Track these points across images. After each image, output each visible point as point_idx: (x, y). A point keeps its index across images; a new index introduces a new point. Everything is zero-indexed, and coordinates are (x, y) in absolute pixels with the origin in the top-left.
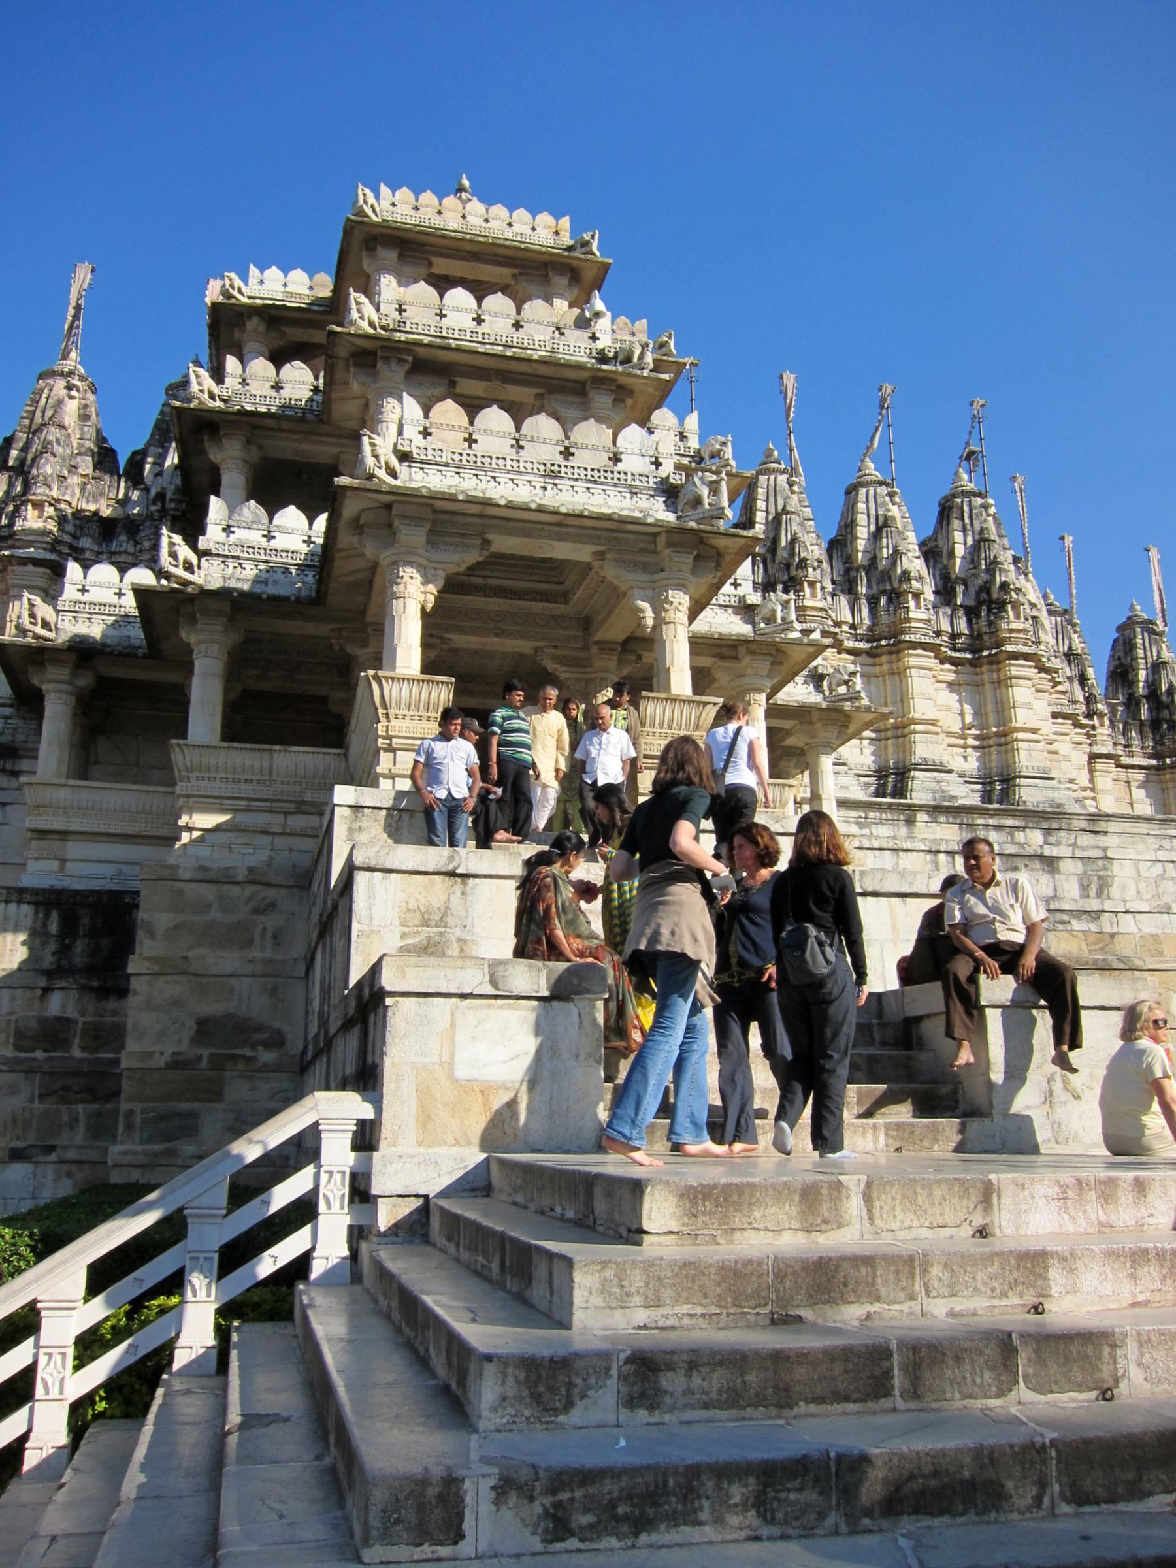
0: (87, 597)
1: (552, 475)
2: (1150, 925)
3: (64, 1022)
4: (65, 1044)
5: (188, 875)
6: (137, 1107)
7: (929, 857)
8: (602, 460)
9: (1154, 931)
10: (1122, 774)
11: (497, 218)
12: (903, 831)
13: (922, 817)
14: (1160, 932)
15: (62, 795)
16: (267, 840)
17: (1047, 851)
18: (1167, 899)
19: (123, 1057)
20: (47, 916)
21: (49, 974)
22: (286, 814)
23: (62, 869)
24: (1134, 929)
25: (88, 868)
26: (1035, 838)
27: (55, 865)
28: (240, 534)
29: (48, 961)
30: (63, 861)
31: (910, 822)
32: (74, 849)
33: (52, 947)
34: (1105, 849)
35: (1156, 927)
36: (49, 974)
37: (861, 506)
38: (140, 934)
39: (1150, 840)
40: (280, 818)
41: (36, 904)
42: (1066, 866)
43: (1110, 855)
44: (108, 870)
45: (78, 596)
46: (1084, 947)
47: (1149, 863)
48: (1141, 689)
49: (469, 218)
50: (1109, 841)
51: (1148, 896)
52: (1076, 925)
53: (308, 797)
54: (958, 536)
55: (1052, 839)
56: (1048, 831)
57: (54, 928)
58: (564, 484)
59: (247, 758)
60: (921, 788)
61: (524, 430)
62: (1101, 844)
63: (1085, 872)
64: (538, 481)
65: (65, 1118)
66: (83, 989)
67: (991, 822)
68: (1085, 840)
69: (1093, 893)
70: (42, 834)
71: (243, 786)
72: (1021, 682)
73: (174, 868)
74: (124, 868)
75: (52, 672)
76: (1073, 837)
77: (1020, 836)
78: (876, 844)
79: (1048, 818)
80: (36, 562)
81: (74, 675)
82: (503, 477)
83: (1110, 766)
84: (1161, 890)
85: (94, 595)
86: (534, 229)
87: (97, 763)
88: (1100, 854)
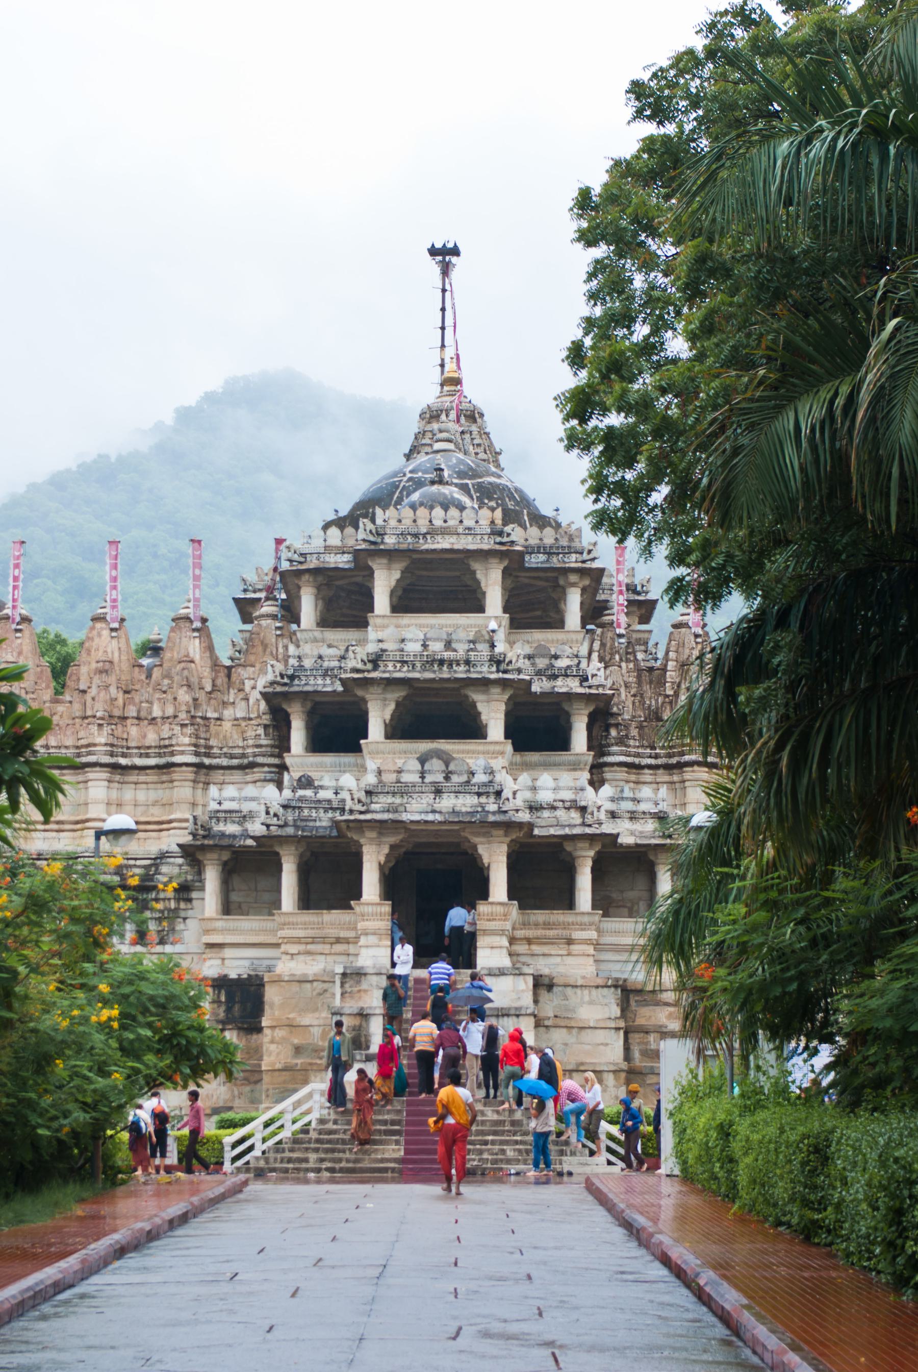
0: (224, 807)
1: (438, 792)
5: (286, 978)
6: (271, 1087)
11: (453, 518)
15: (219, 924)
16: (323, 957)
19: (263, 1063)
20: (219, 993)
21: (223, 1022)
22: (331, 944)
23: (223, 964)
27: (219, 962)
29: (222, 1015)
30: (223, 959)
32: (228, 953)
33: (223, 1008)
36: (223, 1022)
38: (266, 1007)
40: (328, 946)
41: (213, 986)
45: (217, 807)
49: (434, 522)
53: (342, 935)
57: (223, 999)
58: (445, 796)
59: (310, 917)
61: (426, 768)
64: (432, 796)
65: (236, 1093)
66: (239, 1029)
71: (309, 931)
73: (279, 976)
74: (255, 962)
75: (209, 856)
80: (187, 765)
81: (220, 855)
82: (415, 796)
85: (227, 806)
86: (477, 522)
87: (233, 890)
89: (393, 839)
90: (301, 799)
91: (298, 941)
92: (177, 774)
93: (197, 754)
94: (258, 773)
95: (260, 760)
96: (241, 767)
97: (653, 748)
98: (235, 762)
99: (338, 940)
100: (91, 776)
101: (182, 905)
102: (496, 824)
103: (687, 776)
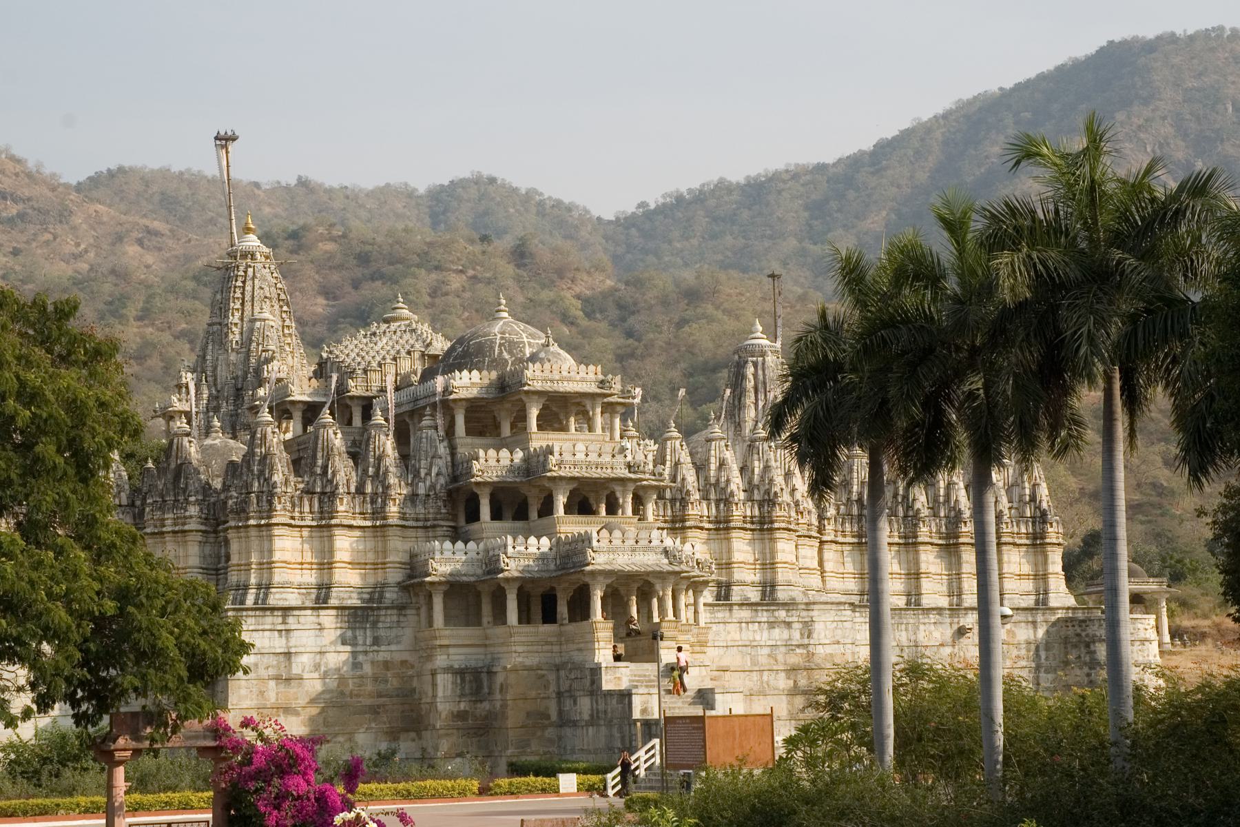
2: (829, 650)
3: (466, 712)
4: (467, 720)
8: (646, 542)
10: (839, 547)
12: (727, 614)
13: (736, 607)
15: (447, 632)
18: (837, 638)
25: (457, 658)
26: (782, 614)
28: (518, 548)
31: (730, 610)
32: (451, 651)
37: (713, 452)
42: (796, 626)
44: (463, 657)
50: (815, 613)
52: (798, 651)
54: (756, 463)
60: (736, 594)
68: (804, 614)
70: (441, 646)
77: (776, 614)
79: (790, 605)
89: (609, 581)
90: (519, 552)
91: (523, 643)
92: (391, 531)
93: (400, 518)
94: (439, 532)
95: (442, 523)
96: (425, 527)
98: (420, 524)
99: (547, 643)
100: (337, 532)
101: (402, 619)
102: (669, 573)
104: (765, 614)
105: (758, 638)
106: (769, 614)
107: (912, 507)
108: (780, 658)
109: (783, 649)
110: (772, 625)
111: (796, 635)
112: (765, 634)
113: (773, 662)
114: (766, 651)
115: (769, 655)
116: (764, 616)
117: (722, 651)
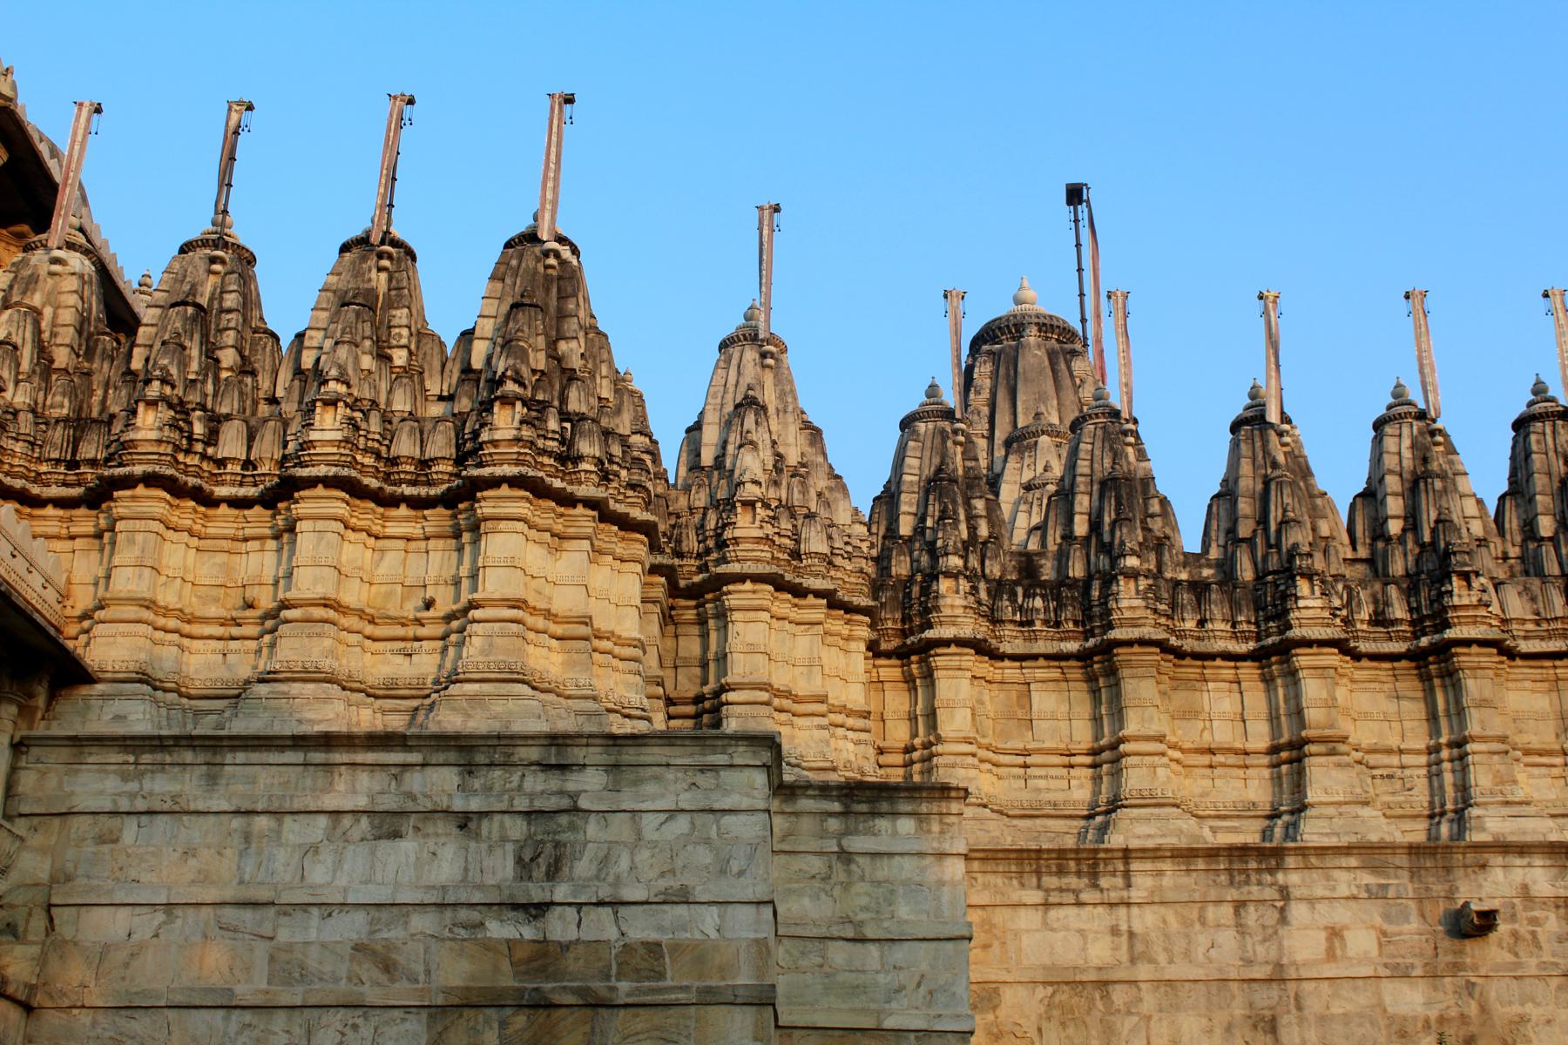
2: (640, 928)
7: (237, 823)
9: (653, 936)
10: (1010, 671)
14: (665, 938)
17: (458, 805)
18: (688, 879)
24: (611, 933)
34: (574, 796)
35: (660, 929)
39: (670, 775)
43: (584, 803)
46: (506, 966)
47: (663, 816)
48: (1081, 527)
51: (652, 874)
52: (499, 929)
55: (477, 784)
56: (469, 769)
62: (571, 786)
63: (530, 836)
67: (168, 759)
68: (536, 782)
69: (539, 872)
72: (503, 525)
76: (516, 778)
77: (415, 781)
78: (141, 805)
83: (969, 659)
84: (679, 863)
88: (565, 803)
97: (73, 464)
103: (120, 509)
104: (364, 779)
105: (318, 873)
106: (379, 781)
107: (1278, 545)
108: (411, 956)
109: (423, 923)
110: (387, 824)
111: (501, 868)
112: (356, 859)
113: (369, 971)
114: (351, 927)
115: (358, 948)
116: (354, 788)
117: (145, 924)
